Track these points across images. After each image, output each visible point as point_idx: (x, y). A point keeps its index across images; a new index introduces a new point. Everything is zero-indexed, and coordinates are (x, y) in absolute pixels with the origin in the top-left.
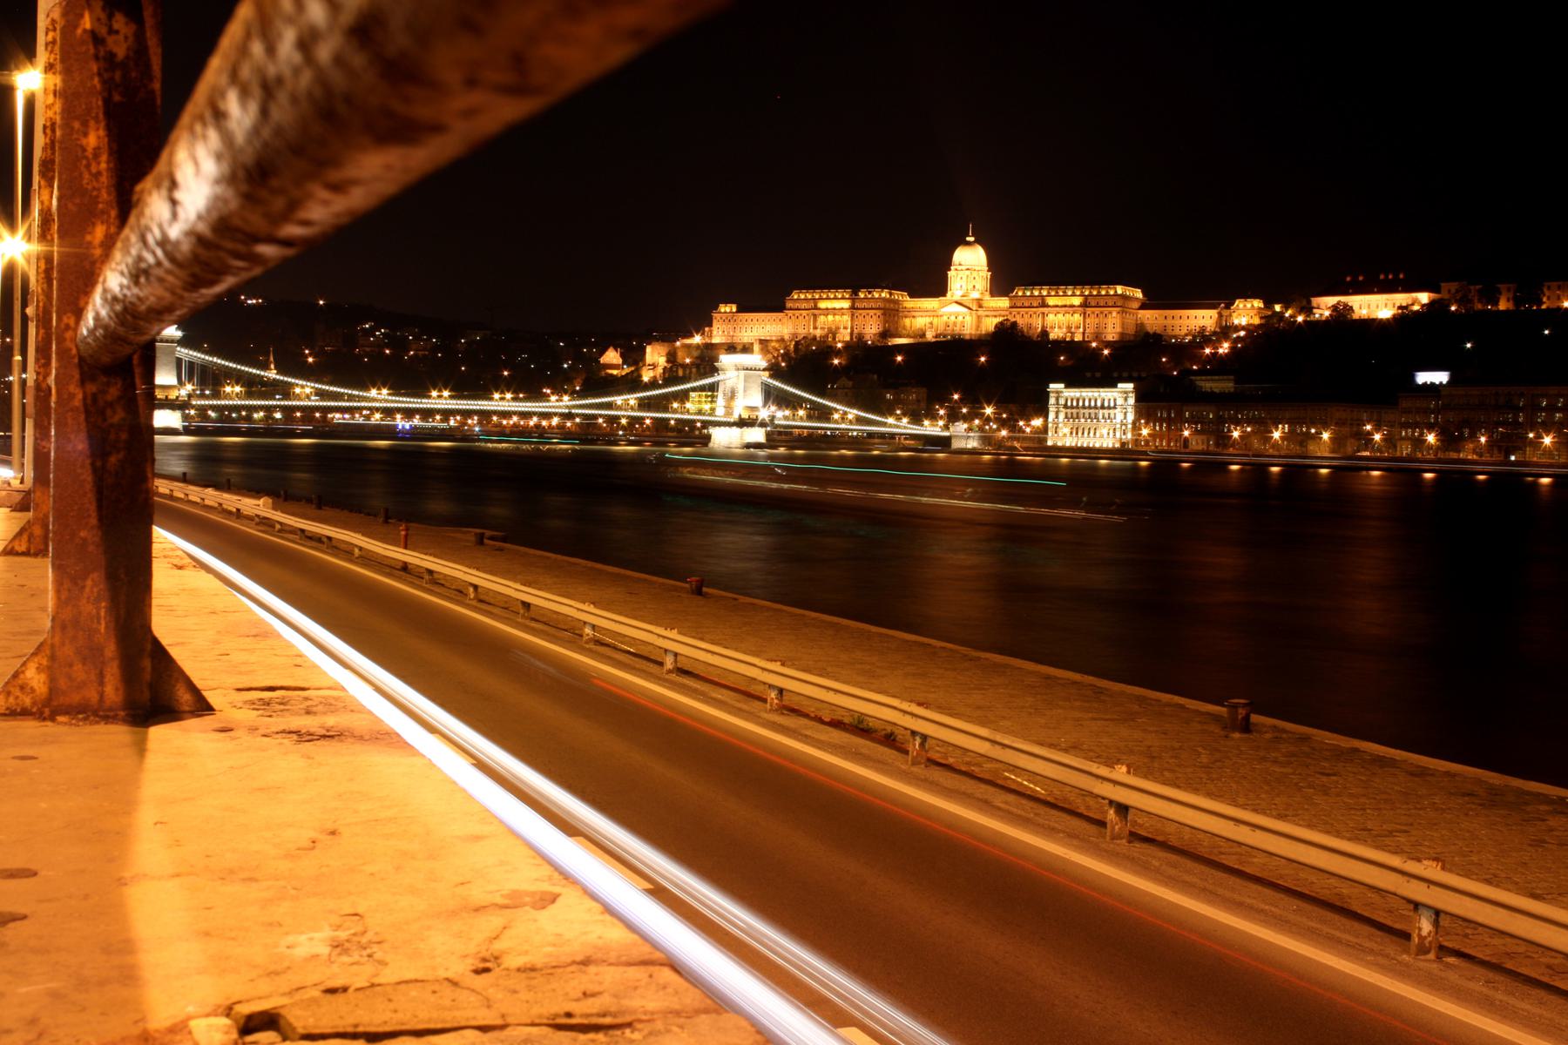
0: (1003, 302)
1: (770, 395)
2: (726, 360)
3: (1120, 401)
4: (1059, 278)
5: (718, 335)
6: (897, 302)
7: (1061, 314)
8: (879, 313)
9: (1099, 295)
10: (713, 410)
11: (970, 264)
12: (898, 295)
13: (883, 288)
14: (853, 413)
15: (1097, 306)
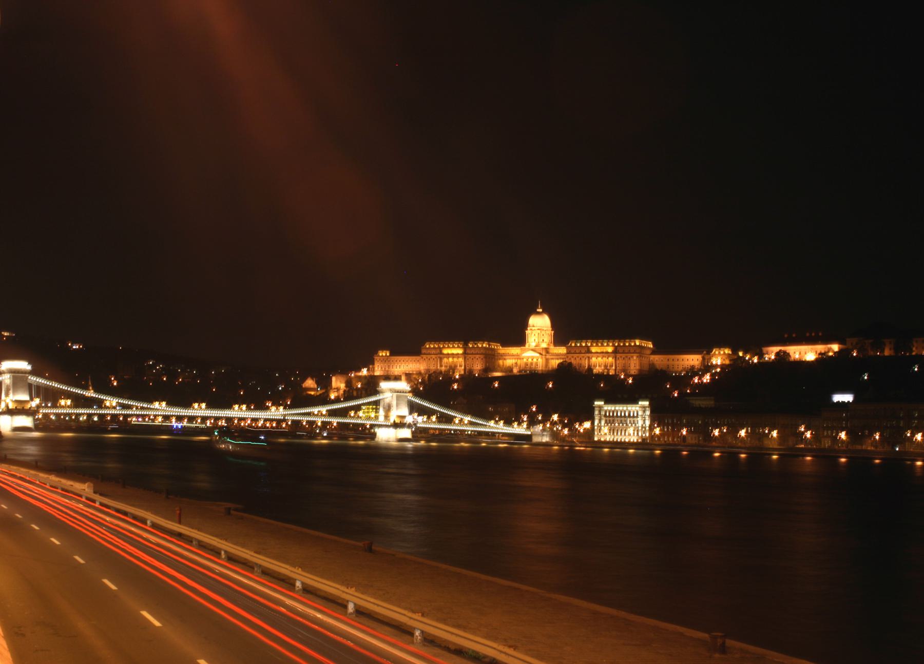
0: (562, 350)
2: (384, 385)
3: (640, 413)
4: (598, 336)
6: (493, 350)
7: (600, 357)
8: (482, 356)
9: (624, 345)
10: (377, 418)
11: (539, 326)
12: (494, 346)
13: (483, 340)
14: (467, 419)
15: (624, 352)
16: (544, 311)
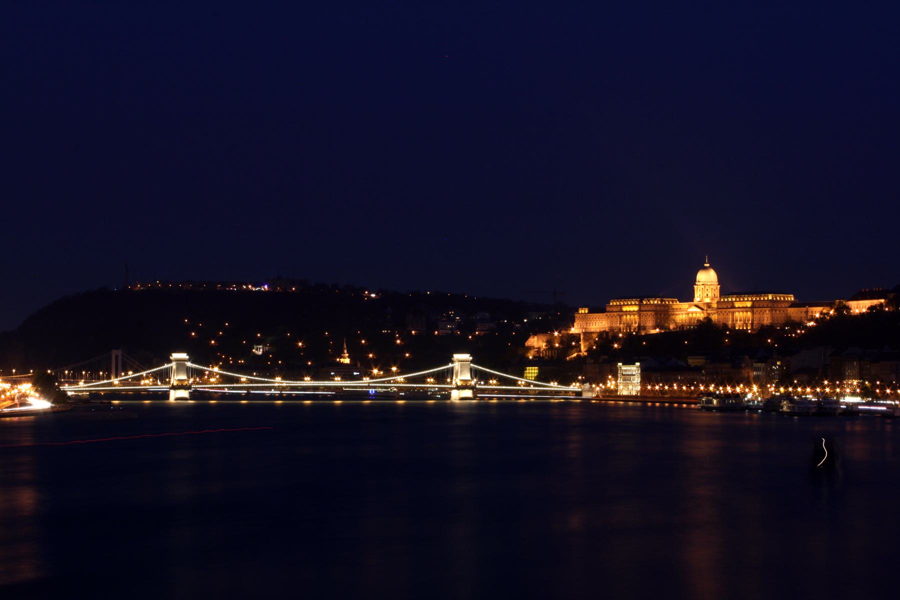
1: (475, 373)
5: (574, 330)
6: (668, 306)
8: (653, 313)
11: (707, 280)
16: (711, 267)
